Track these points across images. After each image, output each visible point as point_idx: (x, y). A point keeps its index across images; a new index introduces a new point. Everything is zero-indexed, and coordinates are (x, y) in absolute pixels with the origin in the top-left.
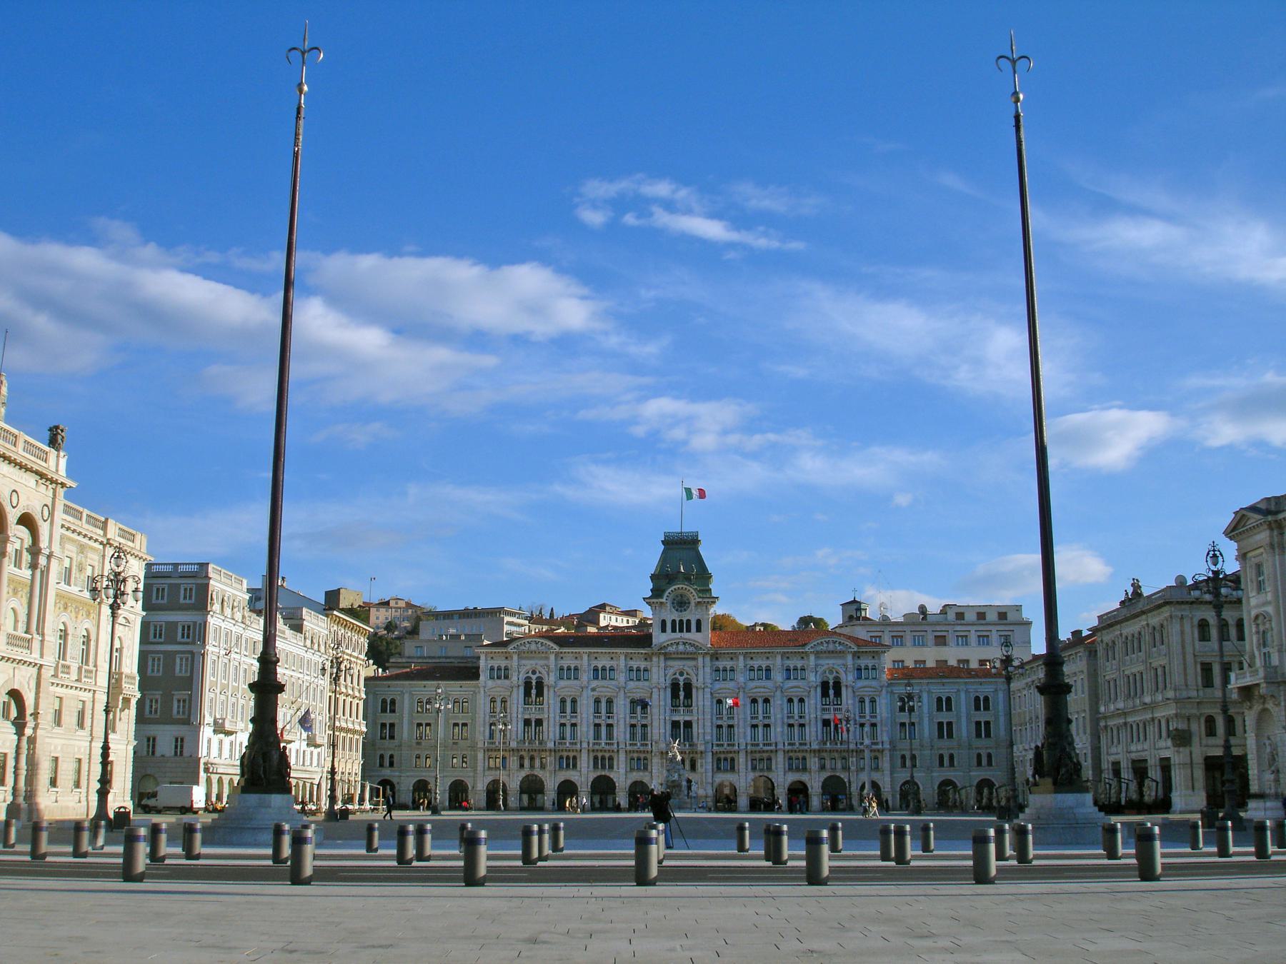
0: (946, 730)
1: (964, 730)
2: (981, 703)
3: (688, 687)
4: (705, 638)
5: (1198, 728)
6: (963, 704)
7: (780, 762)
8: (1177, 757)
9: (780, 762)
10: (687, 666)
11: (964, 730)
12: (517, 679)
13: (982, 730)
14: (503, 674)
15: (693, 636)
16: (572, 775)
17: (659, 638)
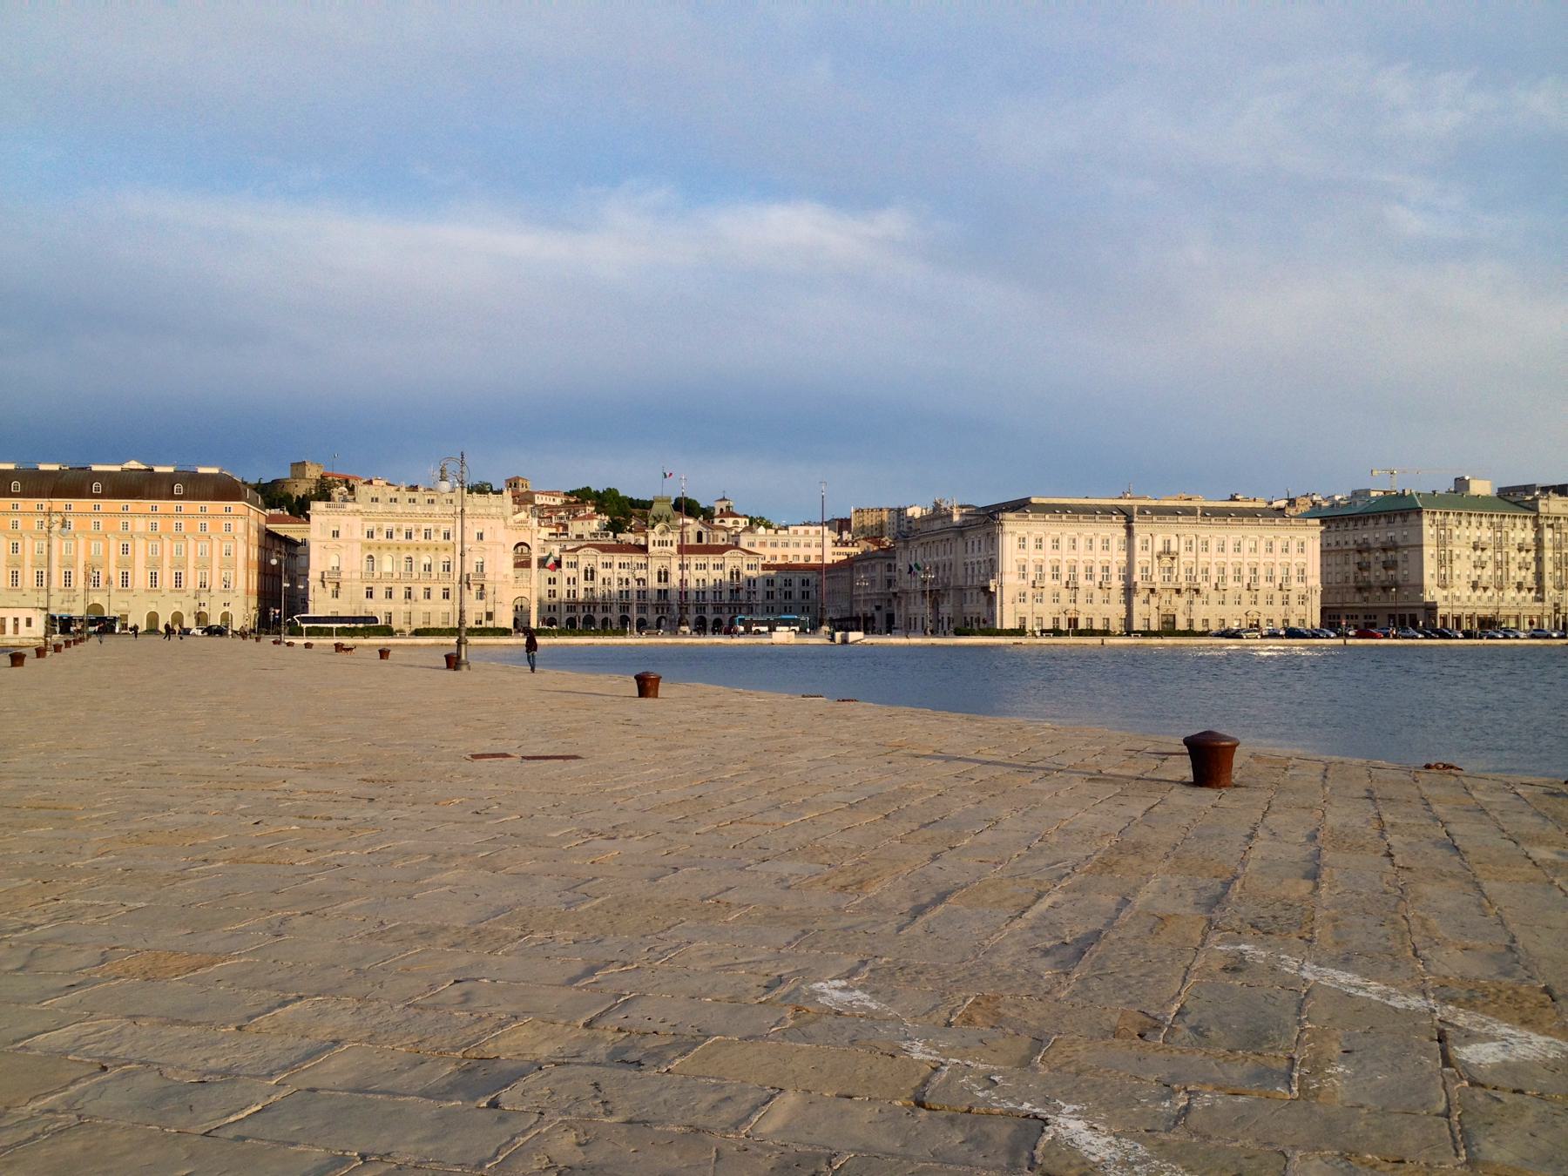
0: (788, 595)
1: (797, 595)
2: (805, 583)
3: (666, 573)
4: (674, 549)
5: (884, 605)
6: (797, 582)
7: (709, 610)
8: (877, 614)
9: (709, 610)
10: (666, 563)
11: (797, 595)
12: (582, 568)
13: (805, 595)
14: (574, 565)
15: (669, 548)
16: (609, 615)
17: (651, 548)
